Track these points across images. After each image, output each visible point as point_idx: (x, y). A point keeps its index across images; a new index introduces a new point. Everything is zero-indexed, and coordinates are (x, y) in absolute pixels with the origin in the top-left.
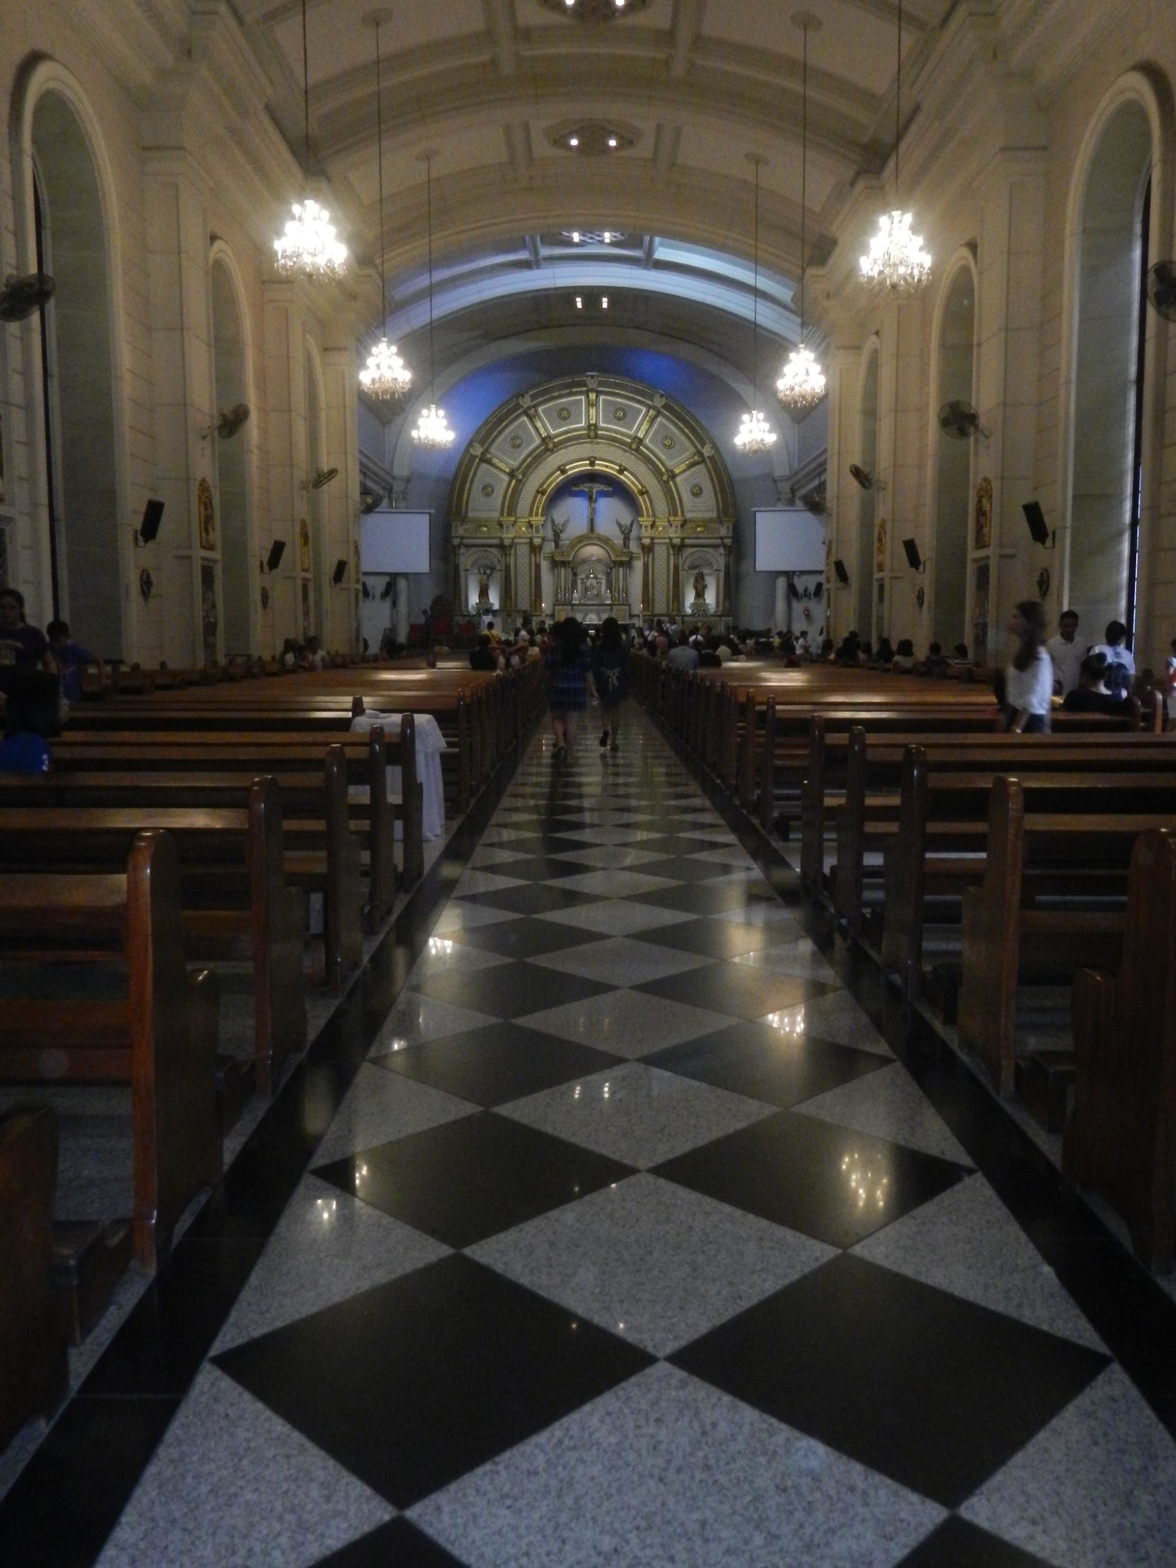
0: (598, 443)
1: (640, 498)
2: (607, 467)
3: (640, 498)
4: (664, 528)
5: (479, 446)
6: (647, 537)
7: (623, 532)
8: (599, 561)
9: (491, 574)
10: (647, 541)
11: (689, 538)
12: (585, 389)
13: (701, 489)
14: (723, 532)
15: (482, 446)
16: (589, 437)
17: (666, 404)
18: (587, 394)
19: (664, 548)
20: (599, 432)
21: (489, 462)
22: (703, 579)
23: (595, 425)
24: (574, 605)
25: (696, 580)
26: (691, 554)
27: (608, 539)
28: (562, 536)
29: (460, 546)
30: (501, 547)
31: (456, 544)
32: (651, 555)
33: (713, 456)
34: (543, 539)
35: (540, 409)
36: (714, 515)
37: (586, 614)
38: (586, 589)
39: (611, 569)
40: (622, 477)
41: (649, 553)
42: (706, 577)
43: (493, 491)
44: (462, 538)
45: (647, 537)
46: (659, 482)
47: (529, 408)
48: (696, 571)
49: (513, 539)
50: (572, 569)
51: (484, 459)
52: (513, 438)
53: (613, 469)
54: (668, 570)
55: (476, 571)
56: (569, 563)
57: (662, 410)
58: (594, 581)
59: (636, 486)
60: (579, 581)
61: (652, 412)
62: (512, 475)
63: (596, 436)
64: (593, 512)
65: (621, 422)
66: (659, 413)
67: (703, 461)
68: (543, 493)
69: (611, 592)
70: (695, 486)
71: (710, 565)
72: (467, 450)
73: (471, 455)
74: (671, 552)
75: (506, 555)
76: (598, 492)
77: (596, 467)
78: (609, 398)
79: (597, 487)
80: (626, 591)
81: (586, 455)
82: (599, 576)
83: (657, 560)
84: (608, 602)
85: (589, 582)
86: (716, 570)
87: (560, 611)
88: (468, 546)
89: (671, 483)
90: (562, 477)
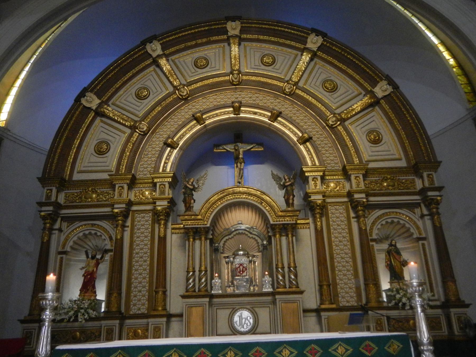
0: (242, 90)
1: (302, 147)
2: (255, 113)
3: (302, 147)
4: (337, 184)
5: (95, 97)
6: (318, 193)
7: (283, 187)
8: (249, 231)
9: (102, 257)
10: (317, 198)
11: (375, 195)
12: (225, 37)
13: (378, 134)
14: (419, 185)
15: (99, 98)
16: (232, 83)
17: (322, 44)
18: (228, 41)
19: (341, 209)
20: (244, 78)
21: (103, 115)
22: (398, 252)
23: (239, 72)
24: (212, 297)
25: (389, 252)
26: (379, 218)
27: (264, 194)
28: (196, 195)
29: (53, 217)
30: (112, 217)
31: (43, 214)
32: (324, 219)
33: (389, 94)
34: (172, 202)
35: (173, 57)
36: (403, 164)
37: (234, 311)
38: (234, 273)
39: (270, 242)
40: (275, 124)
41: (321, 215)
42: (402, 253)
43: (108, 150)
44: (58, 206)
45: (318, 193)
46: (324, 128)
47: (159, 56)
48: (385, 246)
49: (130, 203)
50: (212, 241)
51: (99, 113)
52: (140, 89)
53: (264, 116)
54: (352, 241)
55: (84, 257)
56: (207, 230)
57: (319, 53)
58: (244, 260)
59: (295, 134)
60: (224, 261)
61: (306, 57)
62: (133, 128)
63: (240, 83)
64: (241, 176)
65: (270, 68)
66: (314, 55)
67: (375, 103)
68: (173, 146)
69: (271, 275)
70: (370, 132)
71: (407, 235)
72: (78, 100)
73: (84, 106)
74: (352, 215)
75: (117, 226)
76: (244, 152)
77: (242, 115)
78: (254, 44)
79: (243, 148)
80: (294, 269)
81: (229, 102)
82: (251, 253)
83: (333, 226)
84: (268, 289)
85: (238, 261)
86: (419, 239)
87: (190, 307)
88: (71, 219)
89: (339, 128)
90: (199, 127)
